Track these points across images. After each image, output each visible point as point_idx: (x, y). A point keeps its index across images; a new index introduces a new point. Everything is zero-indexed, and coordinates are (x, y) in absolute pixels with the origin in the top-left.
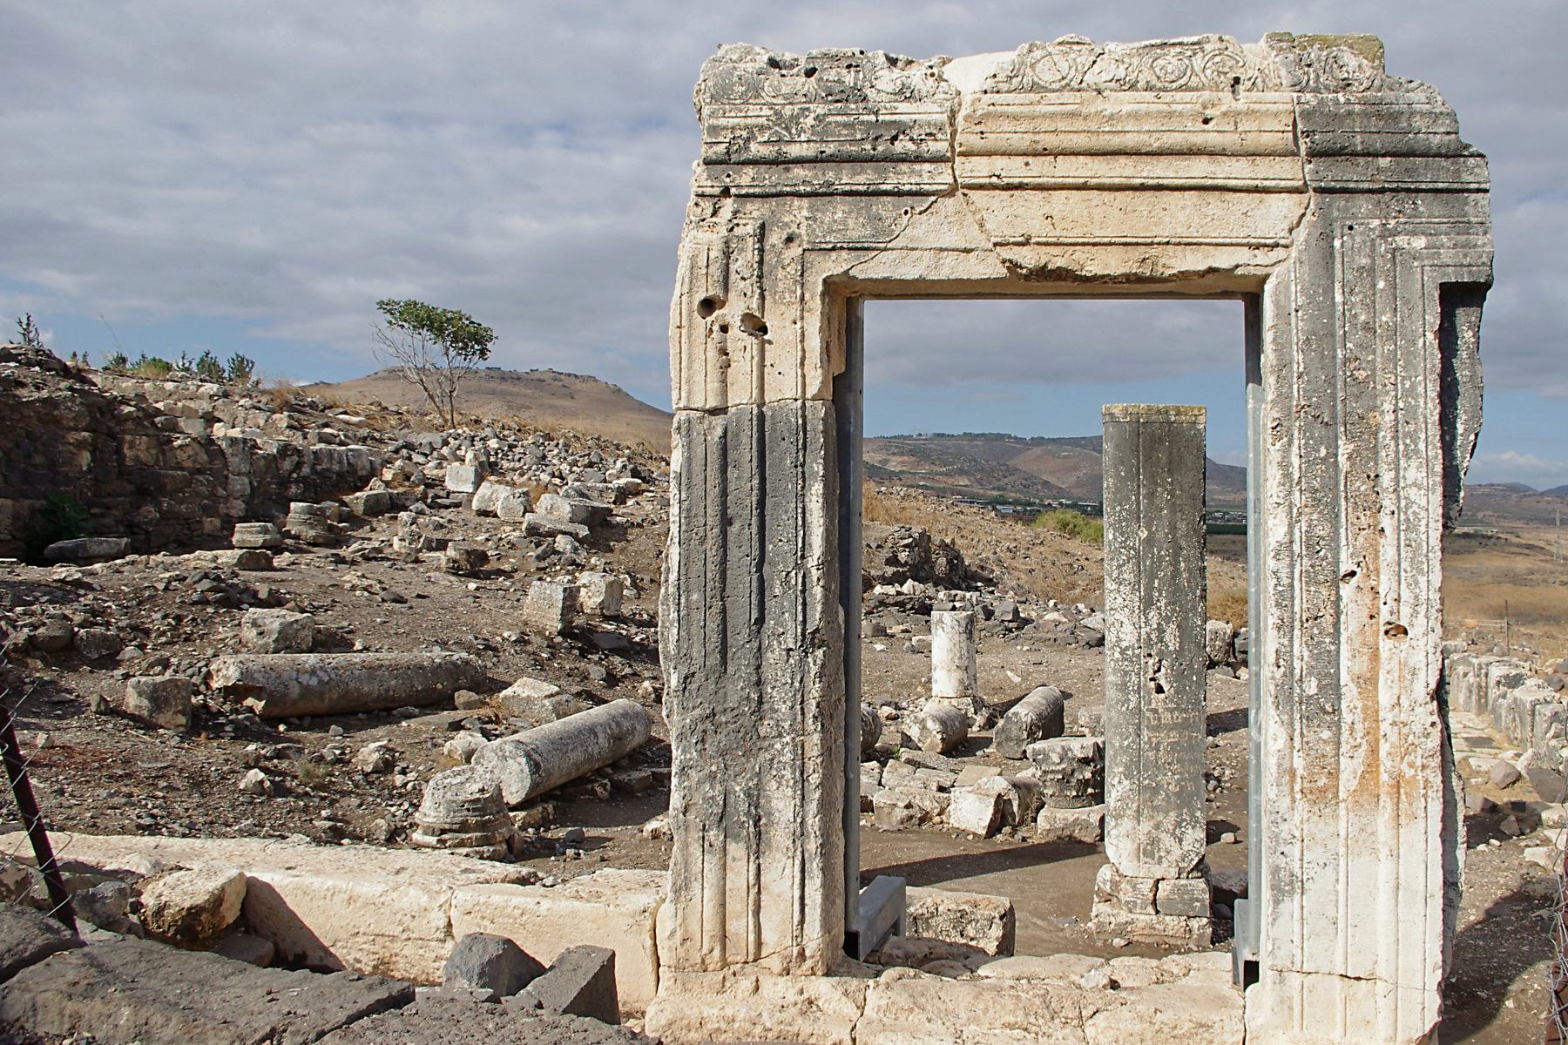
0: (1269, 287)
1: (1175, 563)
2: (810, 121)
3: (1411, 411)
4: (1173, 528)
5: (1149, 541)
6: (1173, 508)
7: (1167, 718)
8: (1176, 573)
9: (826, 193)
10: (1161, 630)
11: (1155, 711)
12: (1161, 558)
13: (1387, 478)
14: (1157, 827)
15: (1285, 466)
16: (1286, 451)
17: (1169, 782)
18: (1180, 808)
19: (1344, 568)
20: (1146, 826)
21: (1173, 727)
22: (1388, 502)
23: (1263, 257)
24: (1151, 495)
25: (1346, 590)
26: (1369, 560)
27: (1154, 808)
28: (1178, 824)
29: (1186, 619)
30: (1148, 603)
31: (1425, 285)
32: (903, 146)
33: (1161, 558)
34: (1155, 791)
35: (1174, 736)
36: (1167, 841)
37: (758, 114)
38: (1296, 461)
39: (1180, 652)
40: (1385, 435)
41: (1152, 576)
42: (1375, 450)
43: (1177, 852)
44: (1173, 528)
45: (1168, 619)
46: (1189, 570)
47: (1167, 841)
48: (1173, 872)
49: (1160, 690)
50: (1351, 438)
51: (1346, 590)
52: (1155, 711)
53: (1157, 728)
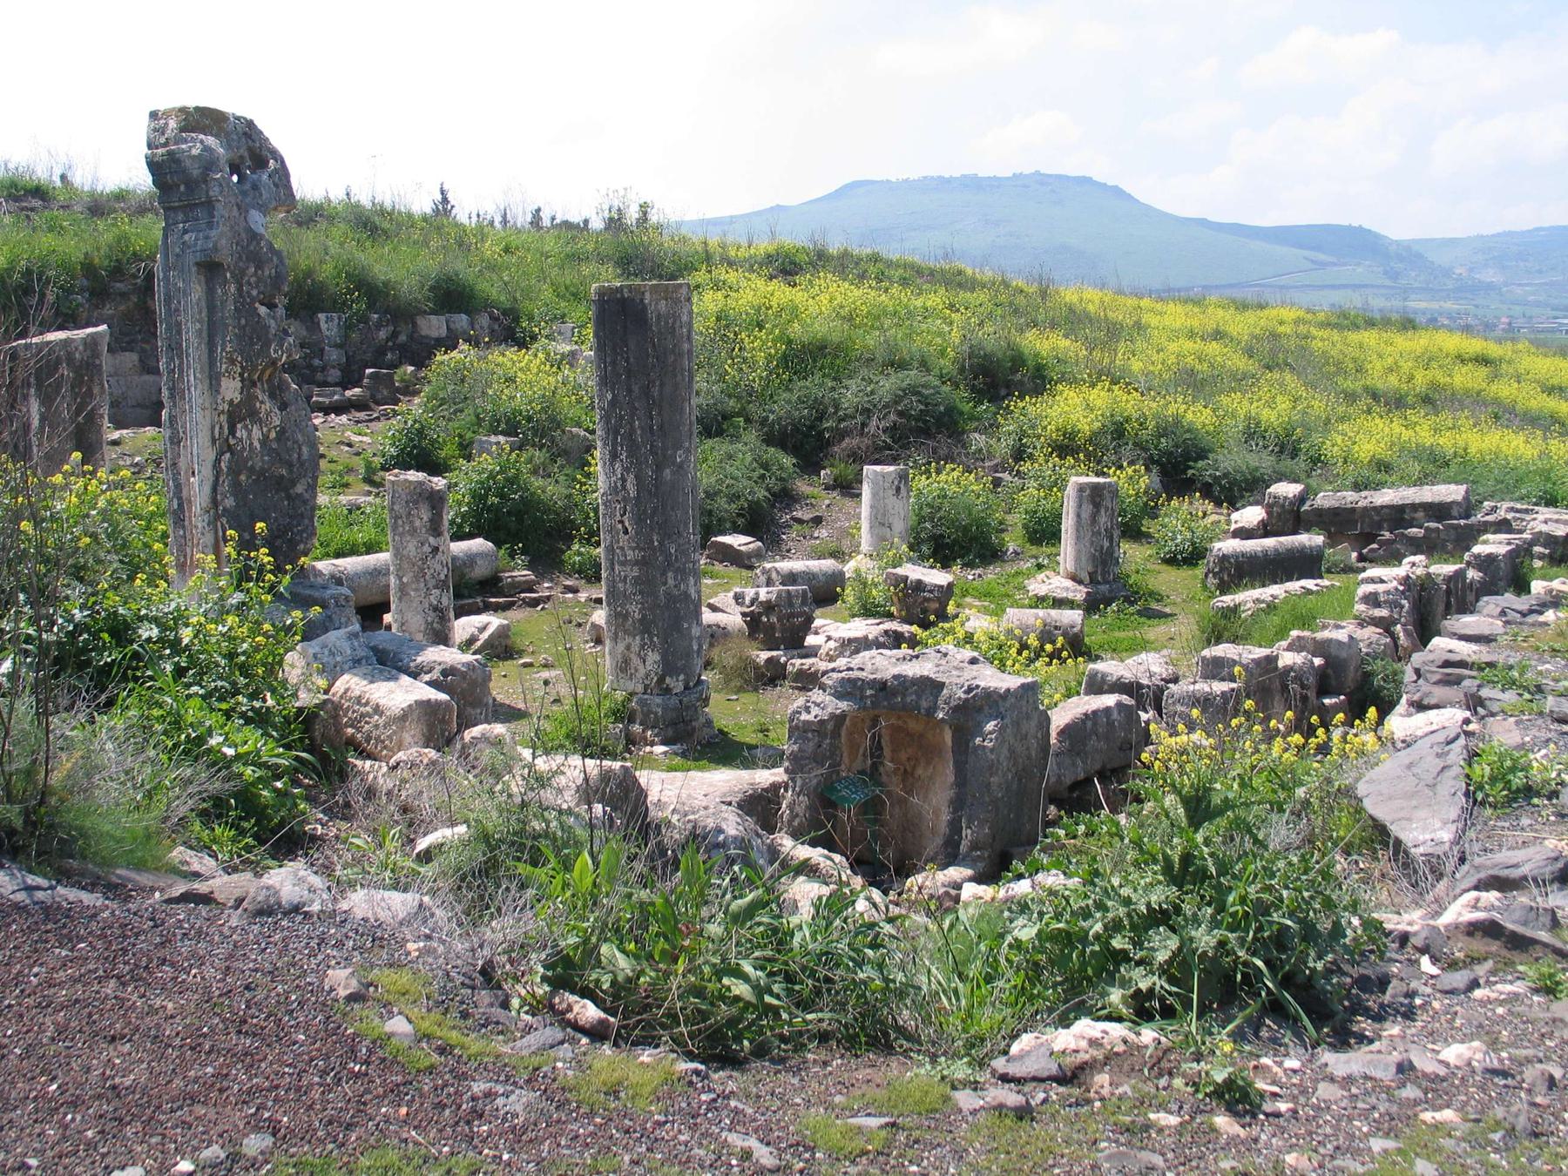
1: (631, 424)
4: (630, 391)
5: (613, 403)
6: (629, 372)
7: (630, 555)
8: (632, 431)
10: (624, 480)
11: (622, 549)
12: (622, 417)
14: (628, 648)
17: (634, 610)
18: (642, 633)
20: (621, 647)
21: (637, 563)
24: (614, 363)
27: (626, 632)
28: (642, 647)
29: (640, 470)
30: (614, 456)
33: (622, 417)
36: (636, 661)
39: (638, 498)
41: (616, 433)
43: (642, 671)
44: (630, 391)
46: (641, 427)
47: (636, 661)
48: (640, 688)
49: (626, 532)
52: (622, 549)
53: (623, 564)
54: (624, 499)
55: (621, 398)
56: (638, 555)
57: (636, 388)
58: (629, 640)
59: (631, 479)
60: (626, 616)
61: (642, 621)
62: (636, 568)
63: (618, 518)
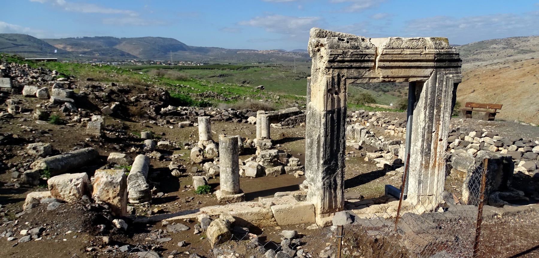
0: (425, 84)
2: (350, 53)
3: (447, 104)
9: (351, 68)
13: (442, 116)
15: (425, 114)
16: (426, 112)
19: (433, 130)
22: (442, 119)
23: (425, 79)
25: (433, 134)
26: (437, 129)
31: (451, 83)
32: (366, 58)
37: (340, 51)
38: (427, 113)
40: (442, 109)
42: (440, 111)
50: (437, 109)
51: (433, 134)
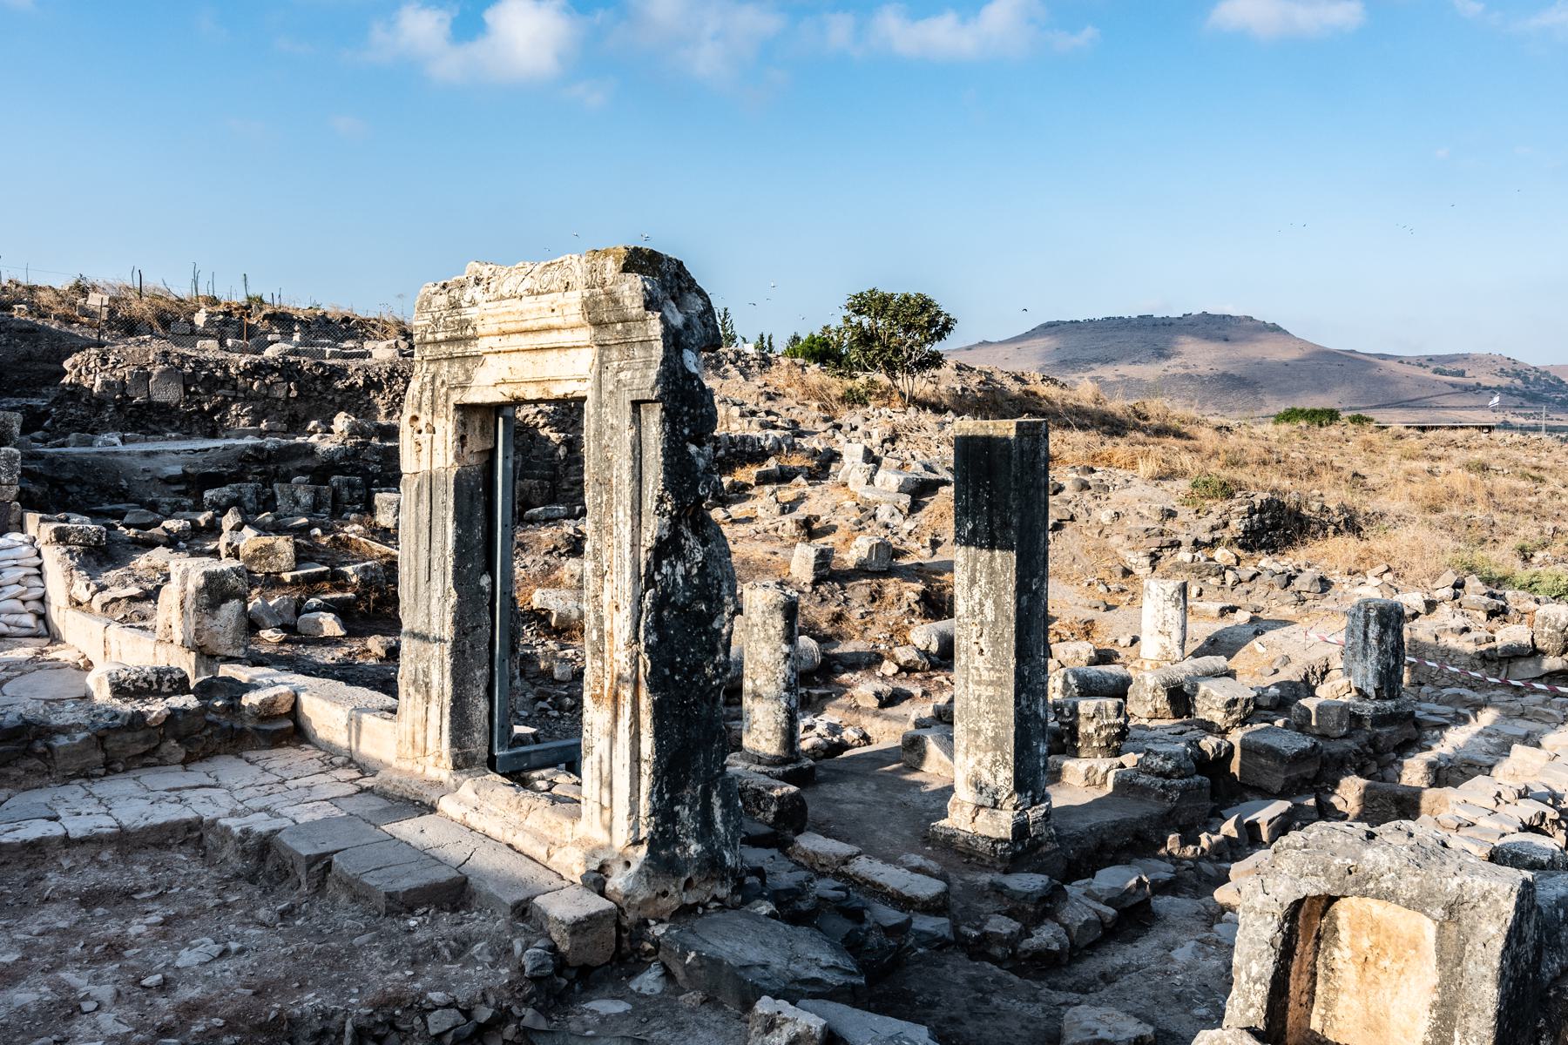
7: (986, 676)
10: (981, 605)
14: (979, 763)
18: (995, 750)
21: (991, 683)
24: (975, 495)
28: (994, 763)
30: (973, 581)
34: (978, 733)
35: (990, 691)
39: (995, 623)
44: (991, 523)
45: (986, 595)
53: (979, 683)
54: (982, 623)
55: (981, 528)
56: (994, 676)
57: (997, 520)
58: (980, 755)
59: (989, 604)
60: (978, 733)
61: (994, 739)
62: (990, 688)
63: (974, 639)
